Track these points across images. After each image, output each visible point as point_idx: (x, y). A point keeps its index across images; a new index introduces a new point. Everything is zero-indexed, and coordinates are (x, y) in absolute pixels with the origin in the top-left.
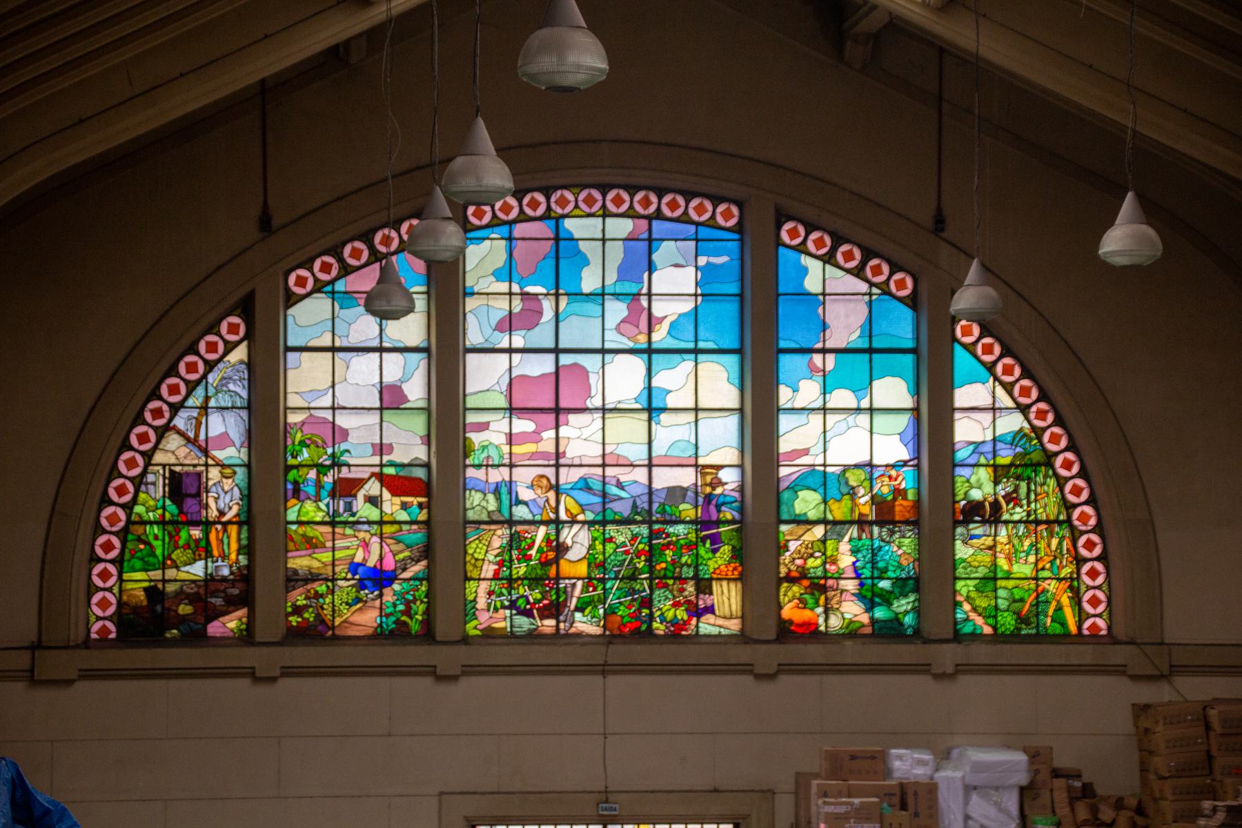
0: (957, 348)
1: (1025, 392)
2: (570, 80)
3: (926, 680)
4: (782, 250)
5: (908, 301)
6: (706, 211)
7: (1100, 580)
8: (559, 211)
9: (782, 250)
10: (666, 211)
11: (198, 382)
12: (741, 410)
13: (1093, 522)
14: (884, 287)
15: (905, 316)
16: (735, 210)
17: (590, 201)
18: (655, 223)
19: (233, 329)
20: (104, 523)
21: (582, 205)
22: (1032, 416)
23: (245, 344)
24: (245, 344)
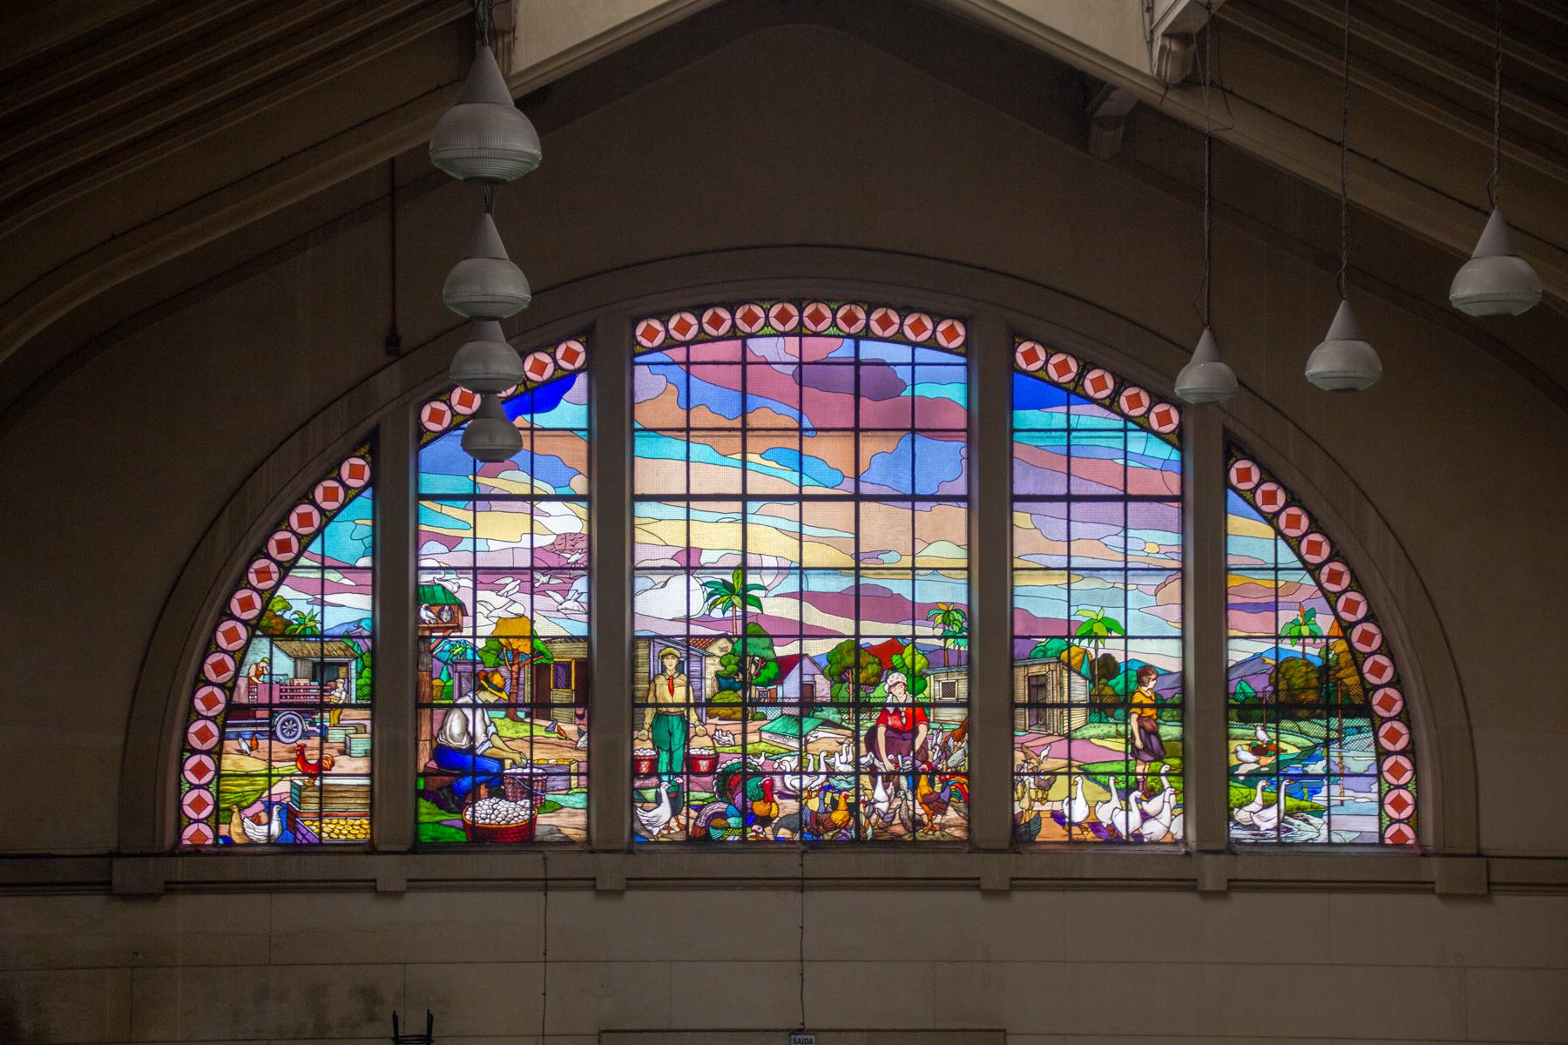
0: (1231, 495)
1: (1314, 548)
2: (494, 169)
3: (974, 897)
4: (1018, 378)
5: (1173, 438)
6: (925, 329)
7: (1407, 777)
8: (747, 329)
9: (1018, 378)
10: (876, 329)
11: (312, 538)
12: (968, 569)
13: (1398, 707)
14: (1141, 421)
15: (1165, 452)
16: (961, 330)
17: (784, 317)
18: (864, 344)
19: (356, 472)
20: (199, 705)
21: (774, 322)
22: (1323, 578)
23: (368, 493)
24: (368, 493)
